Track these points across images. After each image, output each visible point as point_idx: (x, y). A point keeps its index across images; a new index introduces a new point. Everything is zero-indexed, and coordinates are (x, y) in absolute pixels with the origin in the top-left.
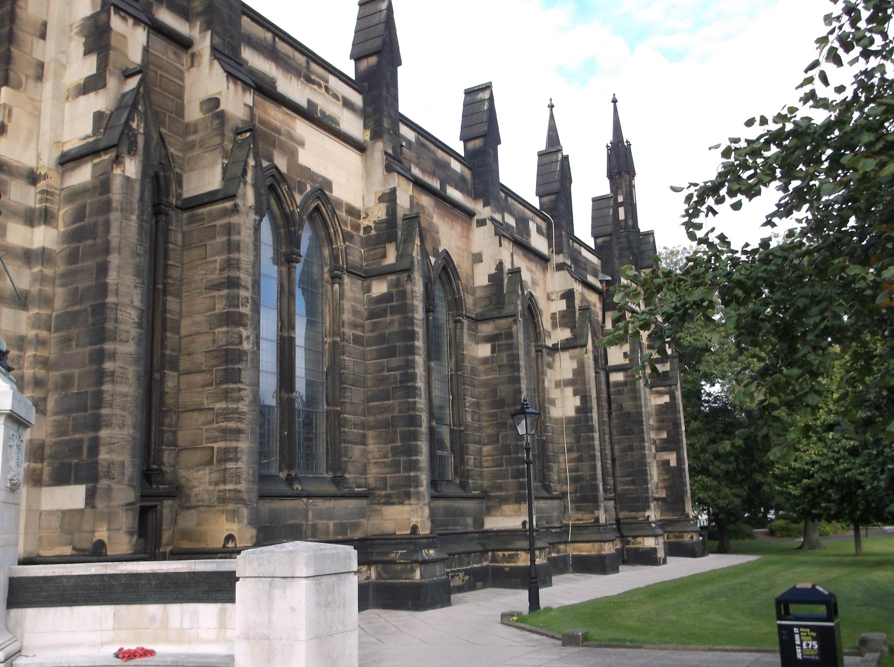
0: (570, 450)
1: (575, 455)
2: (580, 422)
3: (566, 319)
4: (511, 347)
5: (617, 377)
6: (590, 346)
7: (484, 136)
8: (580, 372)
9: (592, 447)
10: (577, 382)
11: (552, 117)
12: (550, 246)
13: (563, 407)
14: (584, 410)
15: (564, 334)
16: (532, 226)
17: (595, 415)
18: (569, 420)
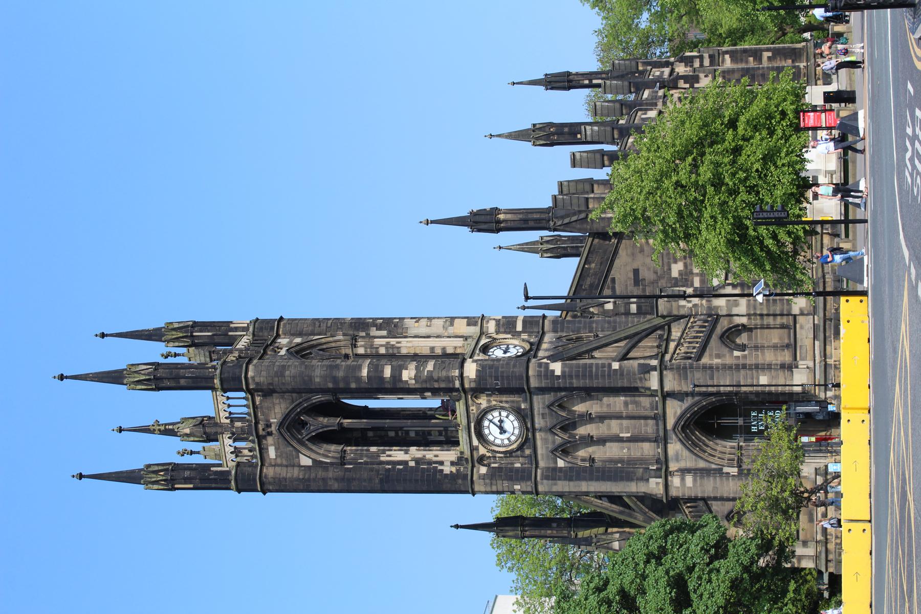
7: (613, 129)
11: (499, 136)
12: (652, 110)
16: (643, 116)
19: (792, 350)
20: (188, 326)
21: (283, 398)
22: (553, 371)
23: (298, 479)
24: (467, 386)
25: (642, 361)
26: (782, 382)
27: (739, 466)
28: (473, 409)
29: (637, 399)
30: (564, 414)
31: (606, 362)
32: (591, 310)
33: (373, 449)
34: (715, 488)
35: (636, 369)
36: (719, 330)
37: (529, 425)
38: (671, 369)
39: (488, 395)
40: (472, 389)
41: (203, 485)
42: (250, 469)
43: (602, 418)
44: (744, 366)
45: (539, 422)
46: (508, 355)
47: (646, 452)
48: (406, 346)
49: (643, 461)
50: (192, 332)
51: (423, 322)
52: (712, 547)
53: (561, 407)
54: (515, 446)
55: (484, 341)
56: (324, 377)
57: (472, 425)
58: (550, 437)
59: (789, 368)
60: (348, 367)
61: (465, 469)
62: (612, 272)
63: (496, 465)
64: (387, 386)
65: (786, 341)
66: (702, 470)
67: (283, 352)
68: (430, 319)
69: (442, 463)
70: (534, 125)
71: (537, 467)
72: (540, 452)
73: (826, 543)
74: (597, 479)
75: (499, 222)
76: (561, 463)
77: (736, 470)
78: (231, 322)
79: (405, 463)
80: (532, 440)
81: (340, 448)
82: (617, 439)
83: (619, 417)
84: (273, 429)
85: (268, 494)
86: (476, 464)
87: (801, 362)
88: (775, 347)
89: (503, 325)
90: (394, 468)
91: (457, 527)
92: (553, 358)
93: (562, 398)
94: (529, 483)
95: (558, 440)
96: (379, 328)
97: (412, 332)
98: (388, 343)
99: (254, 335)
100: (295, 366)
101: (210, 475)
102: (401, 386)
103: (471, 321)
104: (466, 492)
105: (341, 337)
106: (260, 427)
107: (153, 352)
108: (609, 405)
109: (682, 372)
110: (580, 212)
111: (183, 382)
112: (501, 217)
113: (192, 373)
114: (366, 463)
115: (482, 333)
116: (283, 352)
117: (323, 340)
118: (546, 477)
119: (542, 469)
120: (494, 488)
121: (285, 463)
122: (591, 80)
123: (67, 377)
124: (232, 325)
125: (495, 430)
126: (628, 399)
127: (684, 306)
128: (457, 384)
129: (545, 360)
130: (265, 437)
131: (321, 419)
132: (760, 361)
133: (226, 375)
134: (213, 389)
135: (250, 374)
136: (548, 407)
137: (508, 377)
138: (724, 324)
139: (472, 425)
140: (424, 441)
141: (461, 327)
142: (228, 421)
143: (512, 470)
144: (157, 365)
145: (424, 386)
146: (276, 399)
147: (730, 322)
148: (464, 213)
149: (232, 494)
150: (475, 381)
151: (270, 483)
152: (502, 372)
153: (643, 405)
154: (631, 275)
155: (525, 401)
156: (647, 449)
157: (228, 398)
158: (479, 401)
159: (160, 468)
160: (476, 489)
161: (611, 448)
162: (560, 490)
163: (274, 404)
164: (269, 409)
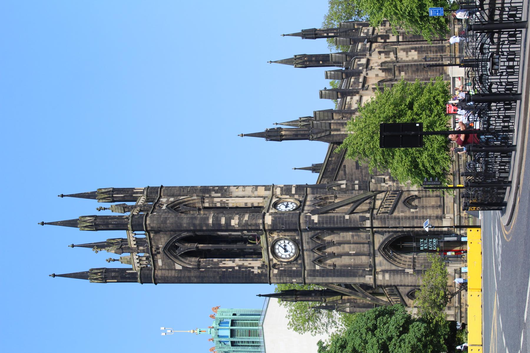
0: (428, 53)
1: (429, 52)
2: (419, 50)
3: (387, 53)
4: (402, 67)
5: (401, 39)
6: (396, 47)
8: (404, 50)
9: (427, 47)
10: (407, 51)
13: (414, 55)
14: (415, 49)
15: (392, 55)
16: (359, 63)
17: (417, 46)
18: (418, 53)
19: (442, 208)
20: (110, 191)
21: (166, 234)
22: (313, 220)
23: (175, 277)
24: (266, 228)
25: (361, 214)
26: (437, 225)
27: (414, 269)
28: (270, 239)
29: (359, 233)
30: (319, 242)
31: (342, 215)
32: (334, 188)
33: (215, 260)
34: (401, 280)
35: (358, 219)
36: (403, 198)
37: (300, 248)
38: (377, 219)
39: (278, 232)
40: (269, 230)
41: (122, 280)
42: (148, 272)
43: (340, 244)
44: (416, 217)
45: (306, 246)
46: (288, 208)
47: (364, 261)
48: (232, 202)
49: (361, 266)
50: (112, 195)
51: (241, 189)
52: (401, 326)
53: (318, 238)
54: (292, 259)
55: (274, 200)
56: (188, 224)
57: (270, 248)
58: (312, 254)
59: (441, 218)
60: (202, 218)
61: (266, 271)
62: (344, 162)
63: (282, 269)
64: (223, 228)
65: (439, 204)
66: (394, 271)
67: (164, 207)
68: (244, 187)
69: (253, 268)
70: (296, 56)
71: (305, 269)
72: (306, 261)
73: (461, 308)
74: (338, 276)
75: (282, 136)
76: (318, 267)
77: (412, 270)
78: (134, 189)
79: (233, 268)
80: (302, 255)
81: (197, 259)
82: (348, 254)
83: (349, 243)
84: (161, 250)
85: (158, 284)
86: (272, 268)
87: (447, 215)
88: (433, 207)
89: (285, 190)
90: (227, 270)
91: (260, 295)
92: (313, 212)
93: (318, 234)
94: (301, 278)
95: (316, 256)
96: (216, 192)
97: (235, 194)
98: (221, 200)
99: (147, 196)
100: (172, 218)
101: (126, 275)
102: (231, 228)
103: (267, 188)
104: (267, 283)
105: (195, 198)
106: (154, 250)
107: (91, 208)
108: (343, 237)
109: (383, 219)
110: (326, 131)
111: (110, 226)
112: (283, 133)
113: (116, 221)
114: (212, 268)
115: (273, 195)
116: (164, 207)
117: (186, 199)
118: (309, 275)
119: (308, 270)
120: (282, 281)
121: (167, 268)
122: (328, 34)
123: (46, 224)
124: (135, 191)
125: (282, 250)
126: (354, 233)
127: (384, 186)
128: (261, 227)
129: (309, 214)
130: (156, 255)
131: (186, 244)
132: (425, 214)
133: (134, 223)
134: (127, 229)
135: (148, 222)
136: (311, 238)
137: (289, 224)
138: (405, 195)
139: (270, 248)
140: (243, 254)
141: (261, 191)
142: (135, 246)
143: (291, 271)
144: (96, 217)
145: (243, 228)
146: (162, 235)
147: (409, 194)
148: (263, 130)
149: (138, 284)
150: (271, 225)
151: (159, 279)
152: (286, 221)
154: (355, 164)
155: (298, 235)
156: (364, 260)
157: (135, 234)
158: (273, 235)
159: (98, 271)
160: (272, 281)
161: (345, 259)
162: (318, 282)
163: (161, 238)
164: (158, 240)
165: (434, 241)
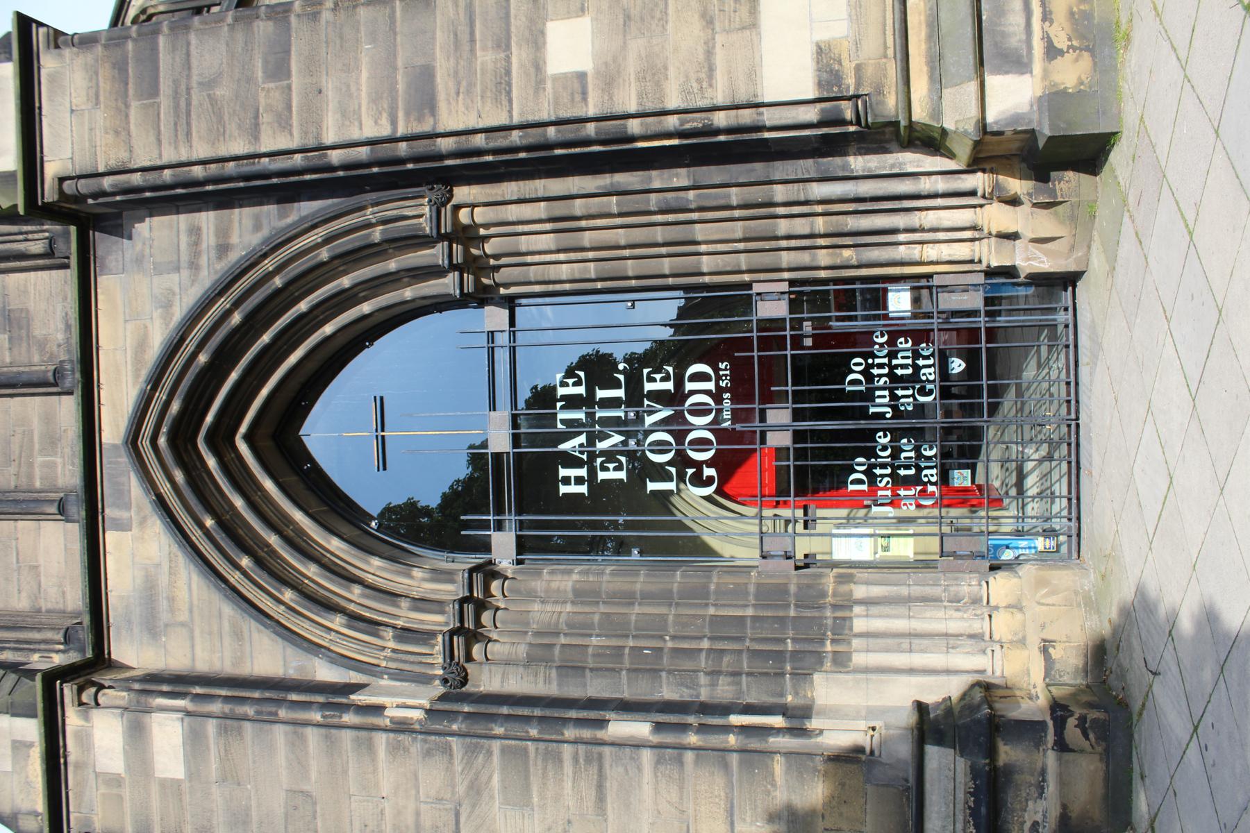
153: (38, 332)
165: (699, 392)
